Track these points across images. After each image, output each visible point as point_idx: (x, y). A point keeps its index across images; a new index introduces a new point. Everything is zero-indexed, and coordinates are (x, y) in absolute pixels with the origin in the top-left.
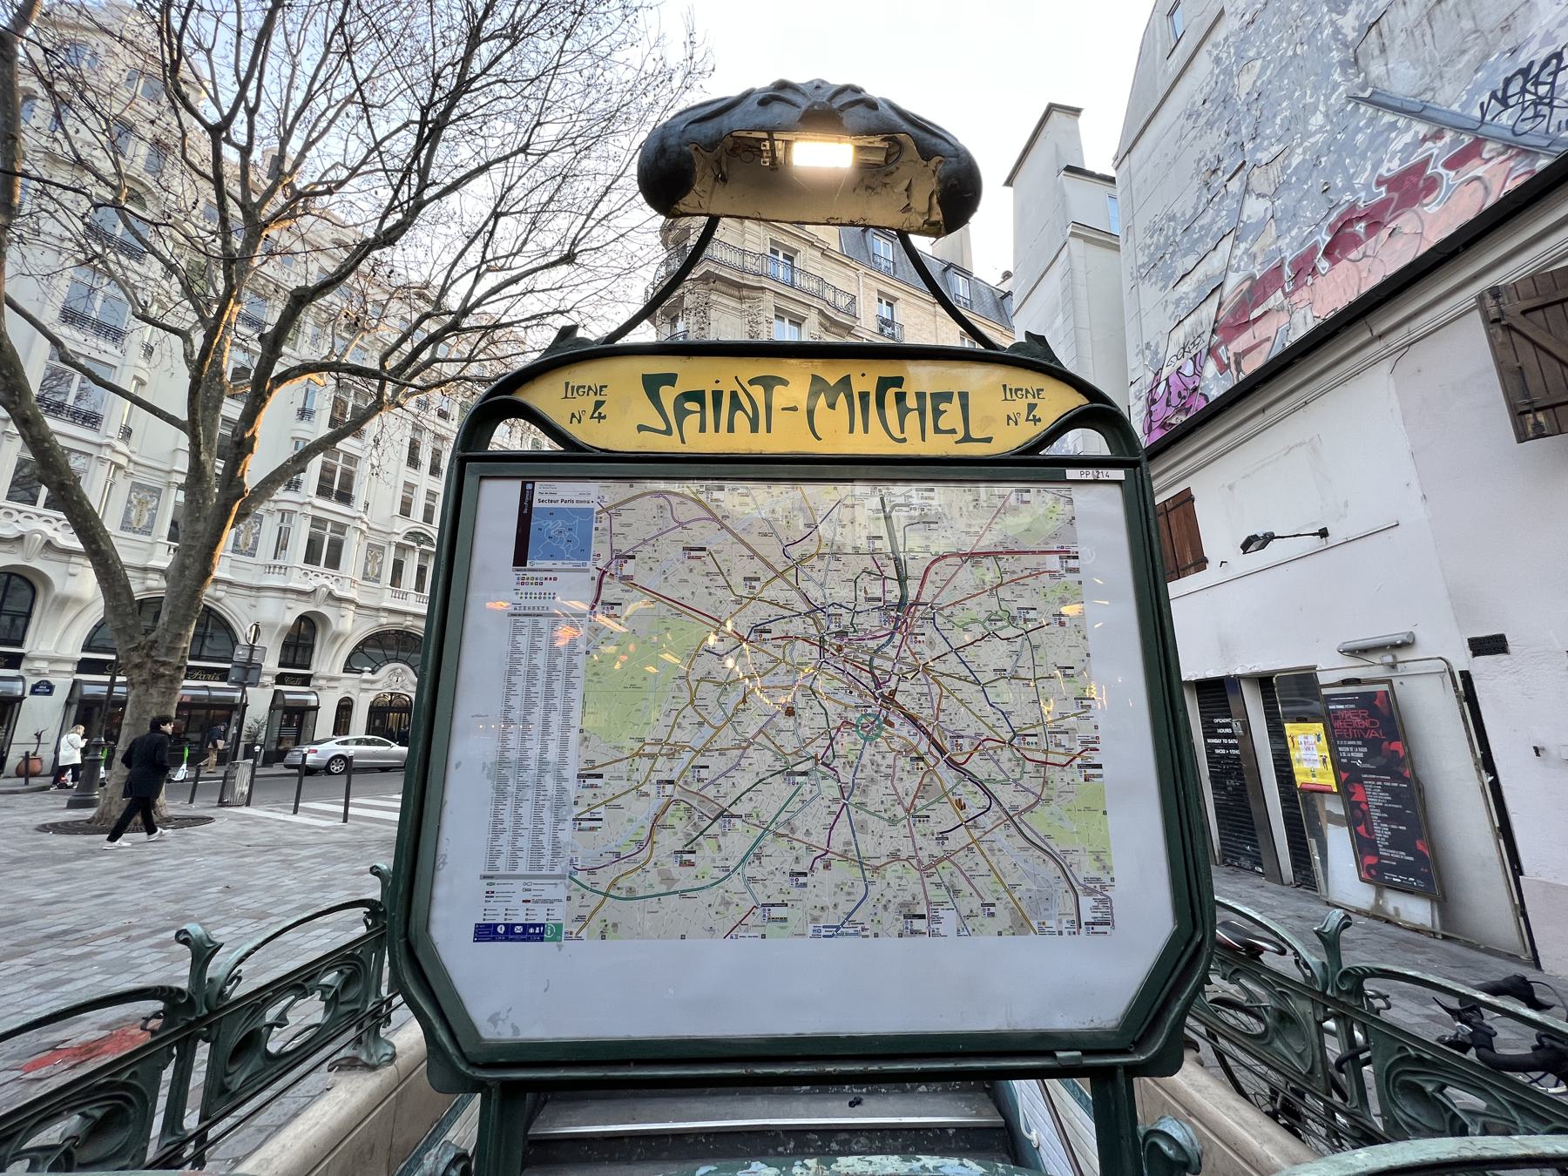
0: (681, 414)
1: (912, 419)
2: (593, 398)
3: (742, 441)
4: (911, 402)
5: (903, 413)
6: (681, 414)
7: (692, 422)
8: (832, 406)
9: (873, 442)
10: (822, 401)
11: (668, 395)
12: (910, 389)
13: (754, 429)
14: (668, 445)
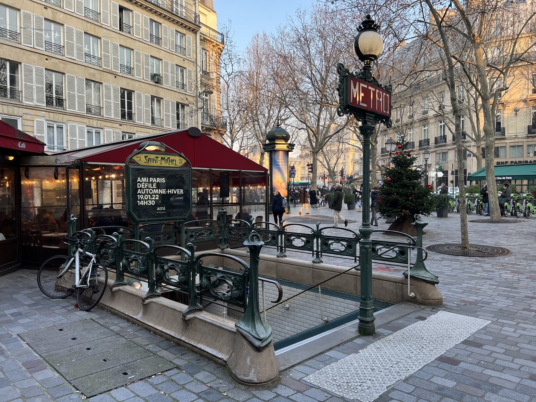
0: (149, 161)
6: (149, 161)
7: (150, 162)
11: (147, 158)
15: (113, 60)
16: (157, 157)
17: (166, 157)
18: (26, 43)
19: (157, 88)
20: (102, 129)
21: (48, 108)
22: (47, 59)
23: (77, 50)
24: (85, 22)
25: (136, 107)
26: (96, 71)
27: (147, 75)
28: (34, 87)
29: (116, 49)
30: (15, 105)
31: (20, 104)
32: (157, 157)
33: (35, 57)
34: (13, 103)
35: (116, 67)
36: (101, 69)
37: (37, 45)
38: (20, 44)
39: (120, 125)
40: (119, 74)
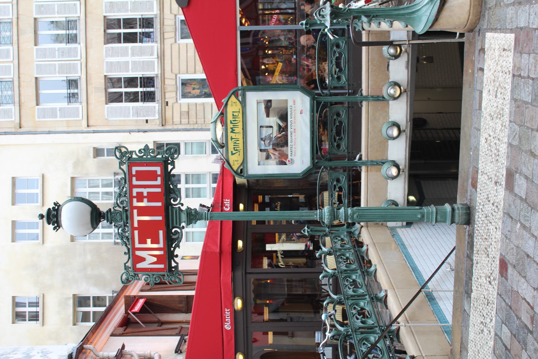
0: (237, 150)
1: (236, 119)
2: (235, 162)
3: (241, 142)
4: (234, 119)
5: (235, 121)
6: (237, 150)
7: (238, 149)
8: (235, 130)
10: (234, 131)
11: (234, 152)
12: (232, 119)
13: (238, 140)
14: (242, 152)
16: (232, 139)
17: (230, 126)
18: (76, 11)
30: (162, 24)
31: (158, 18)
32: (232, 139)
34: (159, 26)
38: (79, 17)
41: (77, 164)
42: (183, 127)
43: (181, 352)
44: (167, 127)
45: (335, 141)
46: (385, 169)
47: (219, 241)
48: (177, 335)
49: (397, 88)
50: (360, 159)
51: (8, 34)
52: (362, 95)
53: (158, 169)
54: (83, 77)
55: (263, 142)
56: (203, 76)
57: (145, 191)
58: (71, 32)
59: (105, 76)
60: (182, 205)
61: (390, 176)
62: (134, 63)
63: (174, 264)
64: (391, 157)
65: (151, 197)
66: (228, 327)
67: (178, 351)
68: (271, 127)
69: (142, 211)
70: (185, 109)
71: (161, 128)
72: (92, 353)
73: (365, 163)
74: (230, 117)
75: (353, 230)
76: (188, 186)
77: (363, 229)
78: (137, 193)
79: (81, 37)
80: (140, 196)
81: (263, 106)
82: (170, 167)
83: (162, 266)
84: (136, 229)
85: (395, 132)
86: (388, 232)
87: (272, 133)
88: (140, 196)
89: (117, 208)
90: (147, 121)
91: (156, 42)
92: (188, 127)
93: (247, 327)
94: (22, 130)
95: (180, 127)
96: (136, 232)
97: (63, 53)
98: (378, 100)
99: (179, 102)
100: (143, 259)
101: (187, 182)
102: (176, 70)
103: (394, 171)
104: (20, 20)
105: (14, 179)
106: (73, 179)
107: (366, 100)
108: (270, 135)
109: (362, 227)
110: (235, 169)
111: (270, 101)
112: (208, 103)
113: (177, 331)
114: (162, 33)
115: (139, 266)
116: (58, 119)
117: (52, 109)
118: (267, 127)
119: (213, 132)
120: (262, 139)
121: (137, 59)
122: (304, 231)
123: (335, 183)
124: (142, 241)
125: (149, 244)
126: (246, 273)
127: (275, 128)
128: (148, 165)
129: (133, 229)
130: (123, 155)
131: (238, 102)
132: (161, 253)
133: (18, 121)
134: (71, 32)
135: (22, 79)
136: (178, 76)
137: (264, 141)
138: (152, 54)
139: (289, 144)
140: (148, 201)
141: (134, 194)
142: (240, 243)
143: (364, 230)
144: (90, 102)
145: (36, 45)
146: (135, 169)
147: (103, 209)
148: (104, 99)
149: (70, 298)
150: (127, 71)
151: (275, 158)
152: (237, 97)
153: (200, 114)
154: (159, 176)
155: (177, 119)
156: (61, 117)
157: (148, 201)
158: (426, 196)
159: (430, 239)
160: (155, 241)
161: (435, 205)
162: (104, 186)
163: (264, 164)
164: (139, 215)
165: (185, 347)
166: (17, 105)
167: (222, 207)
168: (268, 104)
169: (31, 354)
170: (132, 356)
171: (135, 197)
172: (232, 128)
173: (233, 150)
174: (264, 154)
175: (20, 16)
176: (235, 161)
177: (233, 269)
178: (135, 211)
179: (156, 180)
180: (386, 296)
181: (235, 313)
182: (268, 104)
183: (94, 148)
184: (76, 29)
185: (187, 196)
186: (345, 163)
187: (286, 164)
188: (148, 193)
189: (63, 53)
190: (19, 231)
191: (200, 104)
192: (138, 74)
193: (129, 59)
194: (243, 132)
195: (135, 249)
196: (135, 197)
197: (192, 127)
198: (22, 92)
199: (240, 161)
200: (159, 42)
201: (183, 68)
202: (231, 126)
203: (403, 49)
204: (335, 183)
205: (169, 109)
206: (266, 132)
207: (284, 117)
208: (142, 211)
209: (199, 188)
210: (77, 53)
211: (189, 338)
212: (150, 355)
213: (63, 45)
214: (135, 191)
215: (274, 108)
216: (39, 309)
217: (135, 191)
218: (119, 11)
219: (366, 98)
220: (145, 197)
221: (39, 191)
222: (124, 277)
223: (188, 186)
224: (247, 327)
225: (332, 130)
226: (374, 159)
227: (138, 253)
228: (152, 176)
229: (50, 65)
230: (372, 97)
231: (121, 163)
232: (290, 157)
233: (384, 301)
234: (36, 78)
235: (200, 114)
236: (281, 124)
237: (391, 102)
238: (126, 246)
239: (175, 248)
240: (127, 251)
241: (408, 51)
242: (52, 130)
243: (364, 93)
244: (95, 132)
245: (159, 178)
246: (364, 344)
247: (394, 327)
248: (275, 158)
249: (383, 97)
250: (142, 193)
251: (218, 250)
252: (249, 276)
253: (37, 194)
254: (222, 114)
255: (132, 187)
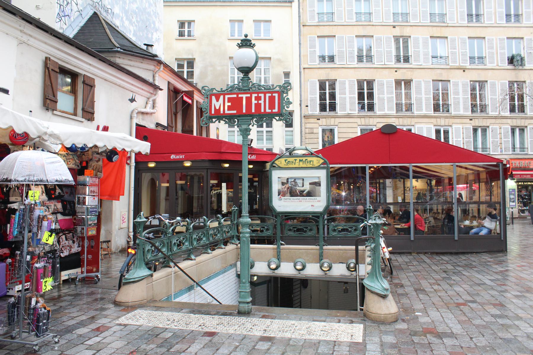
3: (293, 166)
9: (305, 166)
11: (287, 161)
12: (308, 160)
15: (462, 55)
16: (296, 160)
17: (304, 159)
19: (517, 72)
20: (451, 126)
21: (397, 115)
22: (396, 71)
23: (423, 55)
24: (430, 28)
25: (489, 97)
26: (443, 70)
27: (502, 61)
28: (386, 98)
29: (464, 43)
30: (370, 117)
31: (374, 115)
32: (296, 160)
33: (386, 72)
35: (464, 61)
36: (448, 67)
37: (388, 61)
38: (374, 64)
39: (471, 120)
40: (467, 67)
41: (279, 61)
42: (303, 130)
43: (157, 127)
44: (303, 119)
45: (294, 228)
46: (275, 260)
47: (228, 151)
48: (168, 124)
49: (328, 269)
50: (282, 244)
51: (363, 19)
52: (324, 245)
53: (276, 110)
54: (336, 66)
55: (293, 180)
56: (336, 142)
57: (262, 102)
58: (365, 58)
59: (336, 80)
60: (253, 126)
61: (270, 264)
62: (345, 98)
63: (214, 120)
64: (282, 264)
65: (258, 106)
66: (173, 157)
67: (158, 125)
68: (303, 186)
69: (249, 100)
70: (315, 131)
71: (303, 115)
72: (157, 69)
73: (278, 247)
74: (309, 159)
75: (235, 239)
76: (265, 132)
77: (236, 245)
78: (261, 97)
79: (361, 65)
80: (258, 98)
81: (317, 180)
82: (277, 118)
83: (213, 112)
84: (238, 96)
85: (299, 267)
86: (233, 262)
87: (299, 187)
88: (258, 98)
89: (251, 84)
90: (307, 106)
91: (359, 113)
92: (303, 133)
93: (172, 169)
94: (302, 27)
95: (303, 128)
96: (235, 96)
97: (351, 53)
98: (320, 256)
99: (320, 127)
100: (217, 100)
101: (267, 132)
102: (340, 125)
103: (273, 266)
104: (372, 26)
105: (270, 21)
106: (270, 58)
107: (320, 248)
108: (298, 185)
109: (237, 245)
110: (276, 162)
111: (320, 185)
112: (319, 146)
113: (170, 124)
114: (364, 117)
115: (214, 98)
116: (309, 50)
117: (315, 46)
118: (303, 184)
119: (299, 148)
120: (295, 180)
121: (348, 100)
122: (235, 207)
123: (266, 228)
124: (230, 100)
125: (227, 104)
126: (207, 169)
127: (302, 189)
128: (279, 103)
129: (238, 94)
130: (285, 88)
131: (319, 164)
132: (222, 112)
133: (307, 24)
134: (365, 58)
135: (334, 27)
136: (337, 127)
137: (294, 181)
138: (350, 110)
139: (292, 198)
140: (255, 104)
141: (260, 95)
142: (227, 165)
143: (235, 246)
144: (320, 69)
145: (356, 36)
146: (276, 95)
147: (250, 75)
148: (322, 79)
149: (193, 56)
150: (340, 94)
151: (282, 189)
152: (323, 164)
153: (312, 141)
154: (272, 111)
155: (308, 126)
156: (310, 51)
157: (255, 104)
158: (256, 288)
159: (229, 289)
160: (229, 108)
161: (251, 291)
162: (265, 78)
163: (278, 181)
164: (246, 97)
165: (160, 129)
166: (318, 24)
167: (251, 154)
168: (318, 184)
169: (158, 32)
170: (155, 95)
171: (258, 95)
172: (302, 160)
173: (288, 161)
174: (285, 181)
175: (374, 27)
176: (281, 162)
177: (210, 161)
178: (249, 95)
179: (269, 109)
180: (192, 260)
181: (181, 161)
182: (318, 184)
183: (290, 72)
184: (366, 62)
185: (258, 132)
186: (279, 234)
187: (279, 195)
188: (261, 103)
189: (351, 53)
190: (236, 24)
191: (318, 141)
192: (338, 101)
193: (348, 95)
194: (299, 168)
195: (224, 95)
196: (258, 95)
197: (303, 135)
198: (326, 27)
199: (281, 166)
200: (359, 115)
201: (342, 130)
202: (304, 160)
203: (353, 273)
204: (266, 228)
205: (315, 120)
206: (300, 182)
207: (309, 194)
208: (249, 100)
209: (263, 140)
210: (351, 62)
211: (166, 132)
212: (156, 107)
213: (356, 53)
214: (262, 95)
215: (315, 188)
216: (186, 37)
217: (262, 95)
218: (378, 90)
219: (321, 248)
220: (258, 102)
221: (262, 37)
222: (206, 88)
223: (265, 132)
224: (172, 169)
225: (300, 226)
226: (281, 253)
227: (222, 97)
228: (272, 106)
229: (343, 45)
230: (322, 252)
231: (280, 86)
232: (283, 198)
233: (189, 259)
234: (335, 36)
235: (312, 141)
236: (305, 192)
237: (318, 264)
238: (227, 89)
239: (224, 121)
240: (223, 90)
241: (352, 276)
242: (302, 46)
243: (325, 247)
244: (300, 72)
245: (270, 111)
246: (161, 244)
247: (172, 264)
248: (282, 189)
249: (322, 260)
250: (261, 100)
251: (222, 151)
252: (205, 171)
253: (260, 36)
254: (312, 154)
255: (265, 94)
